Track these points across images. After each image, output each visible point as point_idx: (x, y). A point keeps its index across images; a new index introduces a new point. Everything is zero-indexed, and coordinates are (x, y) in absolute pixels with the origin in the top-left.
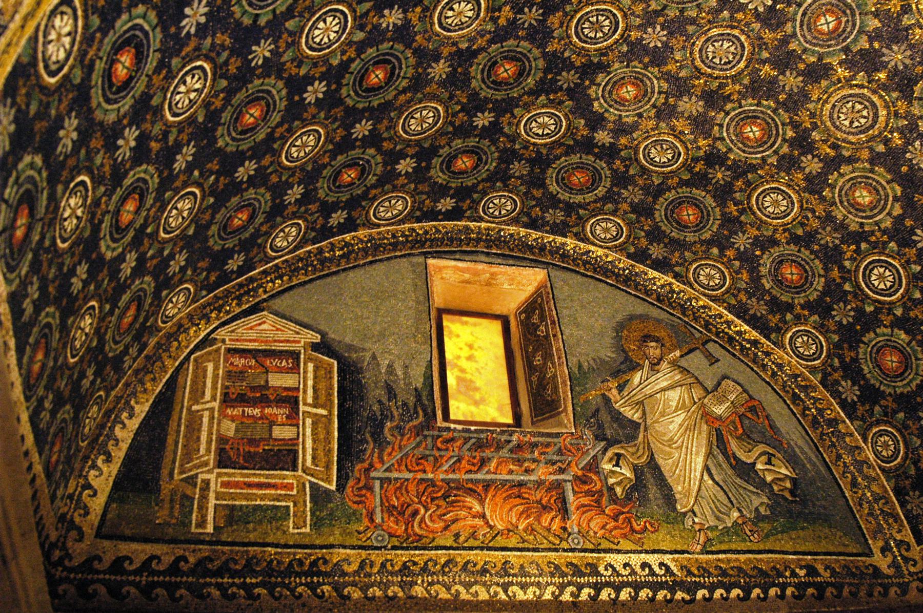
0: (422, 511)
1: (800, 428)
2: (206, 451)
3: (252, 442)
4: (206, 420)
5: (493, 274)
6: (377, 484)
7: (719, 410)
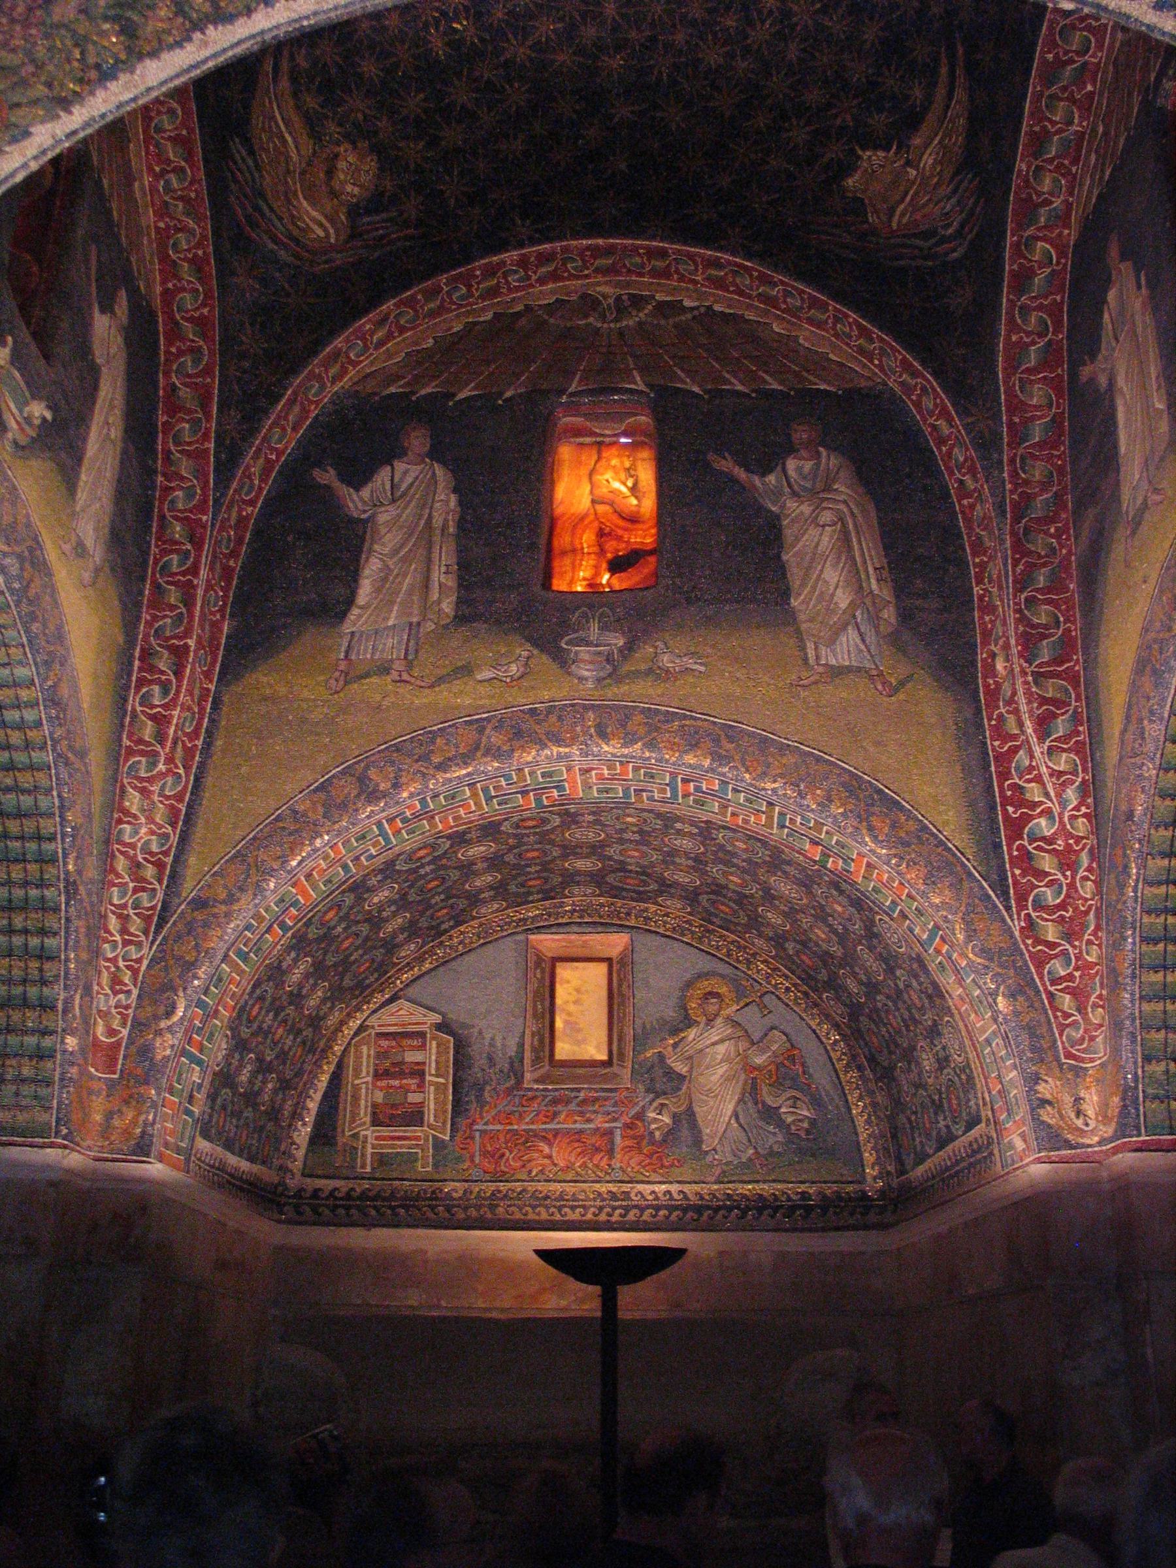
0: (508, 1154)
1: (833, 1073)
2: (365, 1116)
3: (394, 1106)
4: (363, 1091)
5: (585, 942)
6: (477, 1134)
7: (759, 1060)
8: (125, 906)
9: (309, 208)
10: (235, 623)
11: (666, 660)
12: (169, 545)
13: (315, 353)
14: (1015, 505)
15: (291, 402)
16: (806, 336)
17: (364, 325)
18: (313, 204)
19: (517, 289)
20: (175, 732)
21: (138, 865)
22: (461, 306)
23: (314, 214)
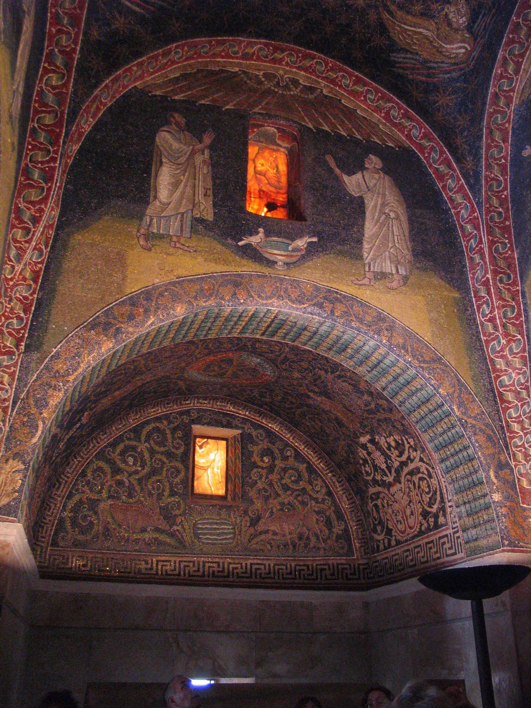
8: (520, 416)
9: (451, 46)
10: (519, 251)
12: (468, 237)
13: (484, 104)
15: (490, 132)
17: (496, 72)
20: (501, 321)
21: (519, 393)
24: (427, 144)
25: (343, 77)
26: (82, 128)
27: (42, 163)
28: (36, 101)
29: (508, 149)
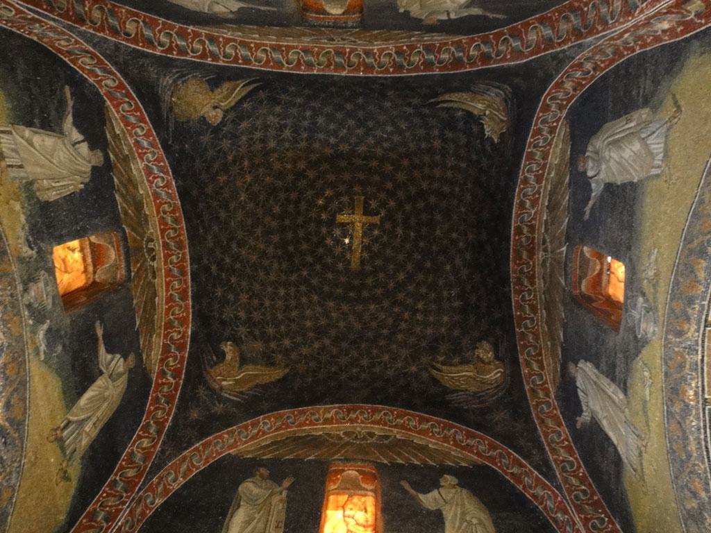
11: (651, 273)
14: (577, 39)
15: (542, 421)
16: (554, 160)
18: (490, 373)
19: (535, 296)
22: (537, 324)
23: (493, 374)
24: (495, 454)
25: (409, 420)
26: (169, 485)
27: (110, 507)
28: (124, 460)
29: (564, 430)
